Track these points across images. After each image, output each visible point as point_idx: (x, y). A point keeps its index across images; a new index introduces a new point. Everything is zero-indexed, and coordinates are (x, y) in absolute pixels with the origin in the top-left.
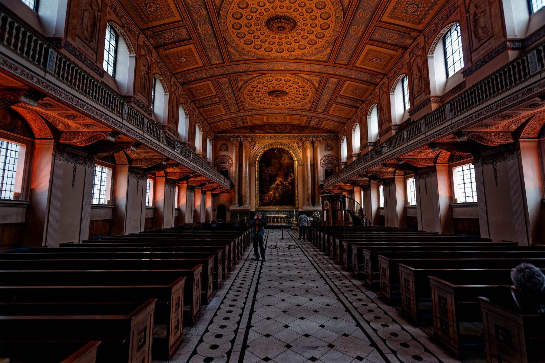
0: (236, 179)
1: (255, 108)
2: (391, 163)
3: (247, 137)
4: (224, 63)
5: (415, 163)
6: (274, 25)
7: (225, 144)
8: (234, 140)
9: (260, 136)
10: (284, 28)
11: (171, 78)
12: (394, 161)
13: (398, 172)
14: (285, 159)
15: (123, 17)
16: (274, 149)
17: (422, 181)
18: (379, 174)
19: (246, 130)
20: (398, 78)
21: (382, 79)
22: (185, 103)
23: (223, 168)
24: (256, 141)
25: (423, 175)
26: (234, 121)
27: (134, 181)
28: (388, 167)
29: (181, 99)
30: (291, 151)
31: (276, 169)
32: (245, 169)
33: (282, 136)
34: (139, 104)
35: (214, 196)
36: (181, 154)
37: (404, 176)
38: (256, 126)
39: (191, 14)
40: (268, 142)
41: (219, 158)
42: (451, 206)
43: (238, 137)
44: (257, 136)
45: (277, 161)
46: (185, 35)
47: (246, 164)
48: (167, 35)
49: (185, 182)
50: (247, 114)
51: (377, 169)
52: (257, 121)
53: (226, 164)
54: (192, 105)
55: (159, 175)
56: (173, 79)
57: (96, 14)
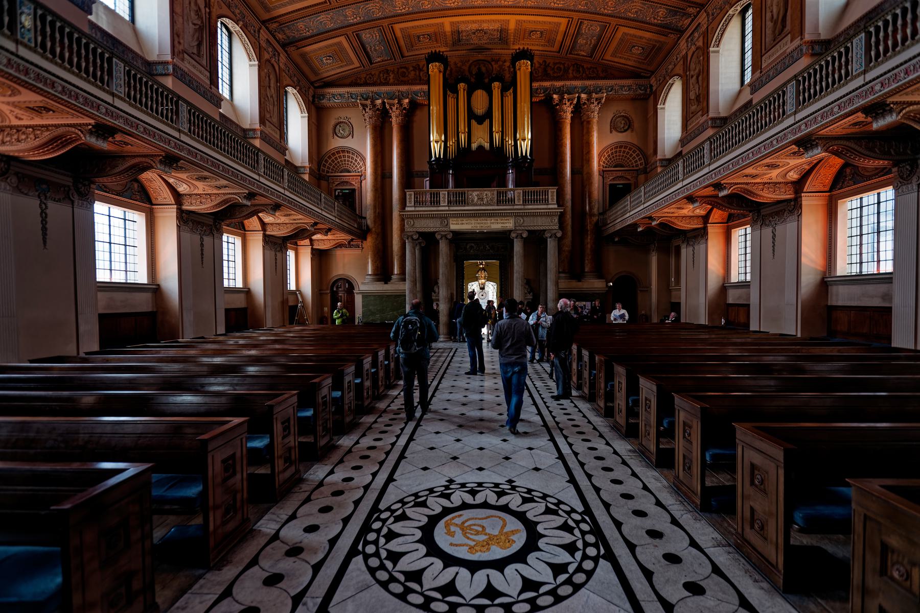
2: (705, 194)
5: (757, 195)
11: (259, 31)
12: (710, 191)
13: (717, 215)
17: (767, 231)
18: (676, 221)
20: (730, 12)
21: (696, 17)
25: (771, 219)
27: (193, 238)
28: (696, 205)
29: (288, 79)
37: (727, 223)
42: (826, 282)
49: (307, 242)
51: (672, 210)
55: (251, 228)
56: (264, 35)
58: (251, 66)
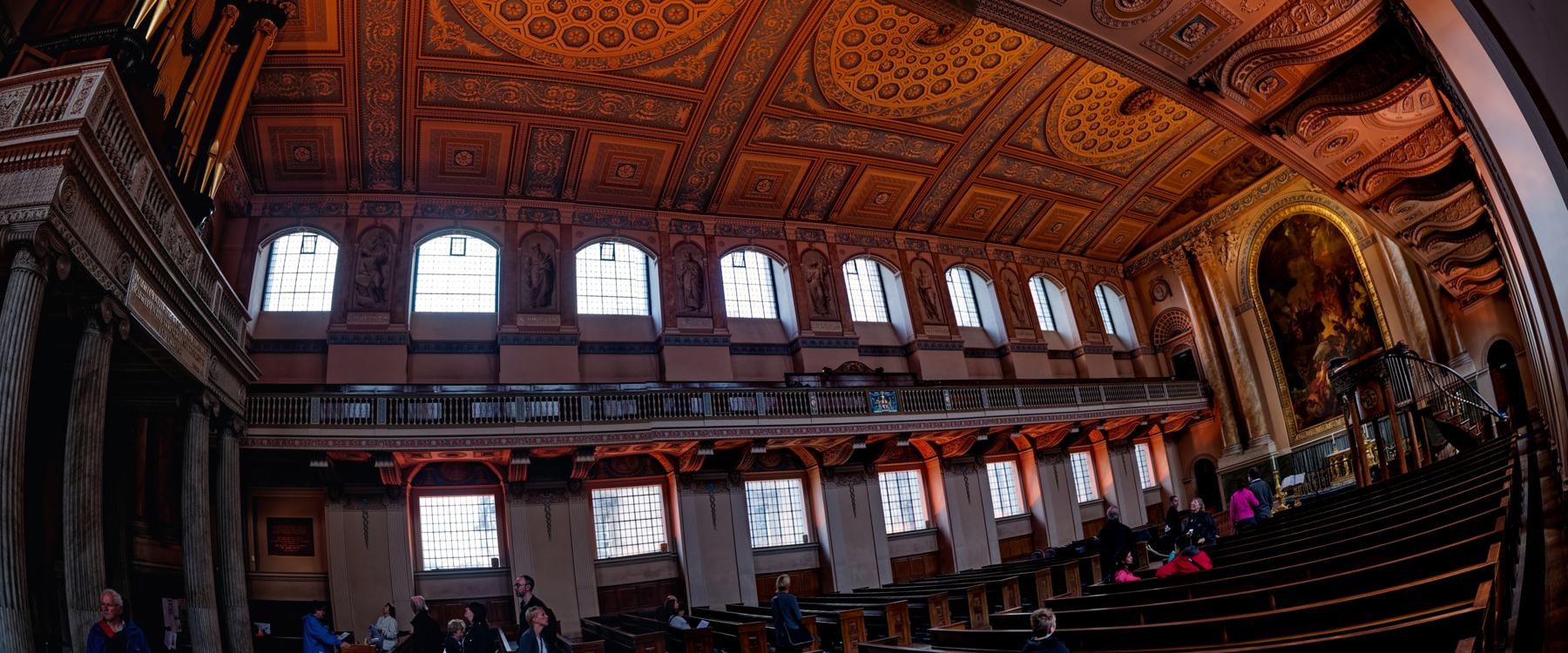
0: (1213, 371)
1: (1146, 156)
3: (1196, 234)
7: (1157, 279)
8: (1170, 258)
9: (1224, 211)
14: (1320, 245)
16: (1279, 228)
19: (1185, 212)
22: (964, 259)
23: (1177, 348)
24: (1223, 230)
26: (1135, 210)
30: (1326, 212)
31: (1311, 288)
32: (1229, 329)
33: (1278, 178)
34: (817, 341)
35: (1168, 439)
38: (1203, 187)
39: (813, 145)
40: (1254, 215)
41: (1159, 326)
43: (1177, 242)
44: (1217, 215)
45: (1302, 261)
47: (1224, 312)
50: (1142, 180)
52: (1191, 182)
53: (1180, 332)
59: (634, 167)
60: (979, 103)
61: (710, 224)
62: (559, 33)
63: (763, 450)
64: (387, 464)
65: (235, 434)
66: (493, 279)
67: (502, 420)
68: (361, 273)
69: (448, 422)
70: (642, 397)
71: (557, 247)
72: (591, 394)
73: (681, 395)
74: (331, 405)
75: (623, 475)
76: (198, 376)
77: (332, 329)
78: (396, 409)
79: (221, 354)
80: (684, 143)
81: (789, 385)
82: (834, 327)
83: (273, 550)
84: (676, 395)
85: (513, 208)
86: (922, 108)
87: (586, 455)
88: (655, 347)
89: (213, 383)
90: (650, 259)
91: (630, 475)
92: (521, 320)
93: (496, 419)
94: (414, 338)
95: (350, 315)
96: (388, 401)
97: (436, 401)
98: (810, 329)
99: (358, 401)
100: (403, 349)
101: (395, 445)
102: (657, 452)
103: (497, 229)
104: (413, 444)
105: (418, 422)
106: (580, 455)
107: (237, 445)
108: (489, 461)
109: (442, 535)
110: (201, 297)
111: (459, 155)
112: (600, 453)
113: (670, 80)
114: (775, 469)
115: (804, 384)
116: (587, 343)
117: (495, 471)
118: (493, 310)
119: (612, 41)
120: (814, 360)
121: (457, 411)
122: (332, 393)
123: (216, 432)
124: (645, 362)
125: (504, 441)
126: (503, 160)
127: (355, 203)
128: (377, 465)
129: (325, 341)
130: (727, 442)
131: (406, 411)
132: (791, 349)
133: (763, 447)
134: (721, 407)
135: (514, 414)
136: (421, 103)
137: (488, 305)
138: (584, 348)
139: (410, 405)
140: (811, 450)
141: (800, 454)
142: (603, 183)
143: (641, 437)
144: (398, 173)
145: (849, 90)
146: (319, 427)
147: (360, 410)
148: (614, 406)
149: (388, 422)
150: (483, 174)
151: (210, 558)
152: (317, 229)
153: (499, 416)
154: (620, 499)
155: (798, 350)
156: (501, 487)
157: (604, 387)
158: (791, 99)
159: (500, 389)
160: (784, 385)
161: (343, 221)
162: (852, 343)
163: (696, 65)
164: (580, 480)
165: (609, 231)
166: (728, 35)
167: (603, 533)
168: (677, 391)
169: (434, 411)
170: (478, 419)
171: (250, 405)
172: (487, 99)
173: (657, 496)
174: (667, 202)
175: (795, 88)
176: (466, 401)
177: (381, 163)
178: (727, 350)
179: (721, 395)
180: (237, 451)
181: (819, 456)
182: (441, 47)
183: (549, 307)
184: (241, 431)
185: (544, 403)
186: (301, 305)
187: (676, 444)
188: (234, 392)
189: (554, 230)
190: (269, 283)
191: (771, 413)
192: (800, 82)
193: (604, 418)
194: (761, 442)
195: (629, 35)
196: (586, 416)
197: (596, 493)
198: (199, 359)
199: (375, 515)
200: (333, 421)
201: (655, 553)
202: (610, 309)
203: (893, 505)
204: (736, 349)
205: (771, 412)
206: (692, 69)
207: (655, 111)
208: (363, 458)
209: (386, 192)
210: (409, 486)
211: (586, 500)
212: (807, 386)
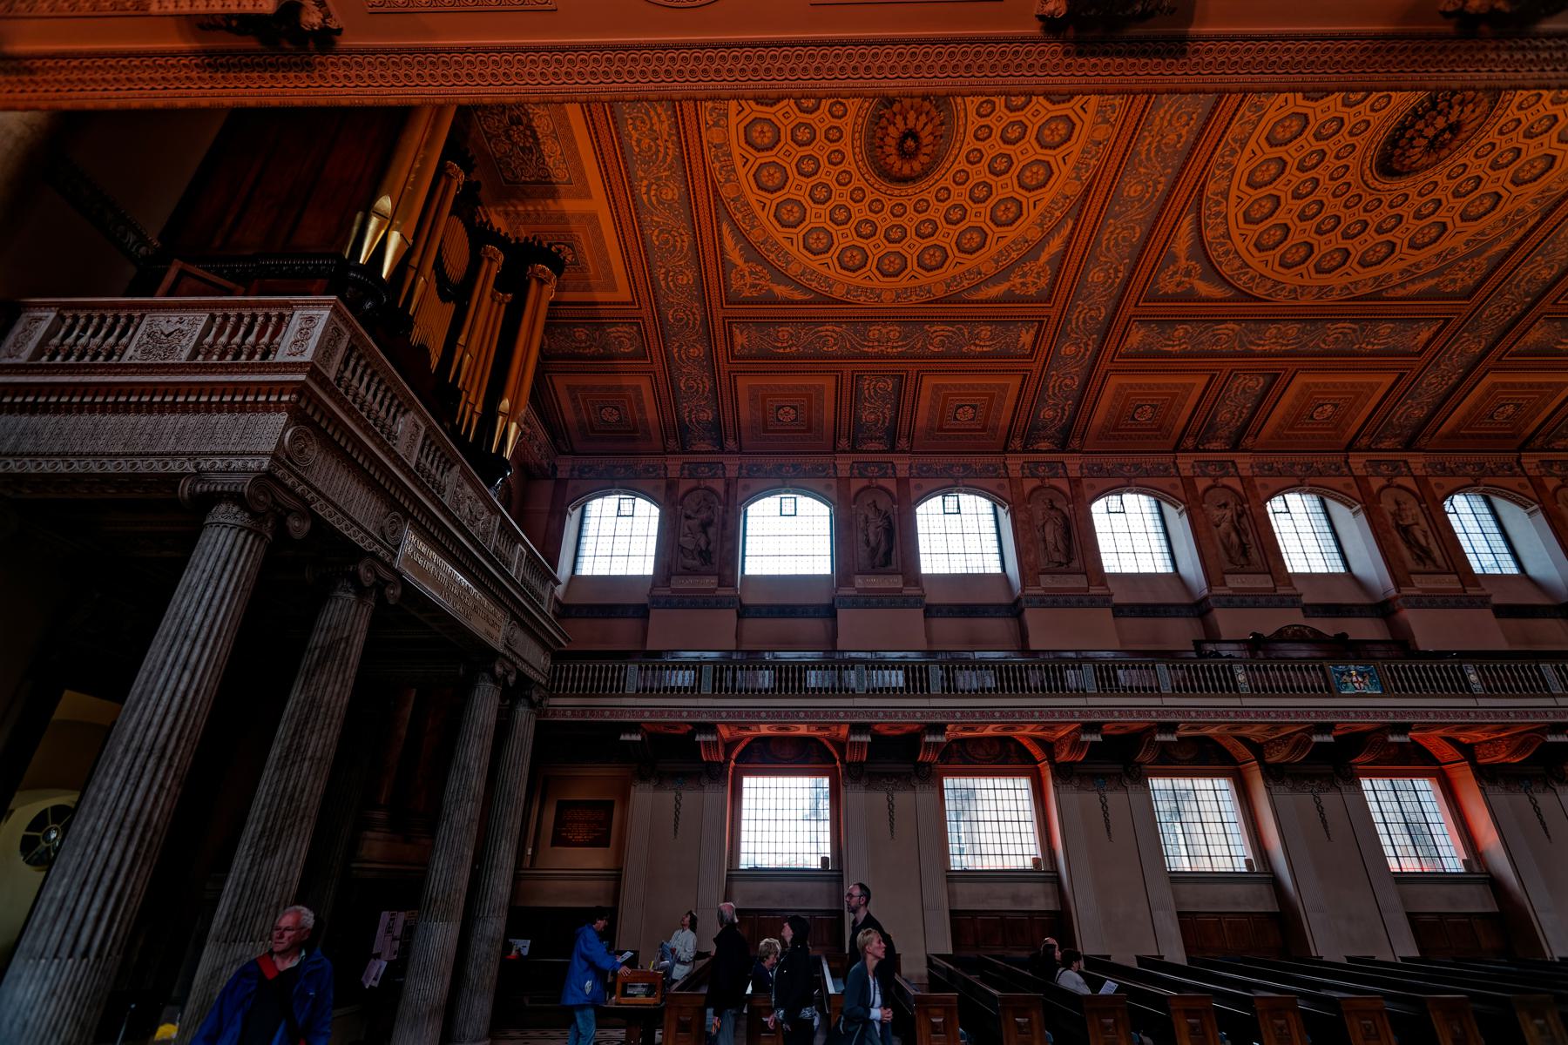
4: (1447, 321)
6: (1407, 162)
10: (1455, 128)
15: (1122, 465)
27: (1301, 800)
36: (1386, 693)
39: (1213, 354)
46: (1257, 384)
48: (1224, 415)
54: (1530, 461)
57: (1066, 510)
58: (1354, 513)
59: (974, 407)
60: (1505, 245)
61: (1074, 464)
62: (872, 263)
63: (1172, 738)
64: (709, 738)
65: (532, 705)
66: (828, 539)
67: (840, 690)
68: (685, 536)
69: (780, 692)
70: (1000, 668)
71: (894, 503)
72: (940, 663)
73: (1053, 667)
74: (650, 673)
75: (982, 762)
76: (492, 643)
77: (654, 593)
78: (723, 678)
79: (522, 619)
80: (1031, 371)
81: (1201, 655)
82: (1262, 582)
83: (559, 840)
84: (1046, 667)
85: (844, 463)
86: (1391, 276)
87: (935, 734)
88: (1014, 610)
89: (510, 650)
90: (999, 509)
91: (988, 761)
92: (859, 582)
93: (833, 689)
94: (744, 602)
95: (674, 579)
96: (715, 669)
97: (767, 668)
98: (1224, 584)
99: (681, 668)
100: (734, 612)
101: (720, 716)
102: (1024, 736)
103: (828, 487)
104: (740, 715)
105: (747, 691)
106: (930, 734)
107: (533, 717)
108: (824, 737)
109: (766, 817)
110: (501, 563)
111: (781, 411)
112: (952, 733)
113: (1009, 298)
114: (1190, 762)
115: (1224, 654)
116: (932, 605)
117: (833, 750)
118: (828, 572)
119: (934, 263)
120: (1231, 623)
121: (790, 680)
122: (653, 659)
123: (508, 702)
124: (997, 627)
125: (842, 714)
126: (828, 414)
127: (674, 465)
128: (698, 738)
129: (645, 605)
130: (1120, 725)
131: (734, 679)
132: (1199, 609)
133: (1173, 733)
134: (1107, 682)
135: (853, 684)
136: (734, 357)
137: (822, 565)
138: (931, 611)
139: (739, 674)
140: (1245, 740)
141: (1229, 744)
142: (940, 429)
143: (1002, 715)
144: (719, 433)
145: (1267, 272)
146: (636, 695)
147: (684, 678)
148: (967, 678)
149: (714, 691)
150: (809, 429)
151: (471, 853)
152: (635, 491)
153: (837, 685)
154: (978, 792)
155: (1210, 610)
156: (837, 768)
157: (955, 655)
158: (1171, 289)
159: (837, 656)
160: (1194, 655)
161: (663, 483)
162: (1293, 601)
163: (1038, 273)
164: (929, 764)
165: (951, 482)
166: (1075, 224)
167: (957, 834)
168: (1044, 661)
169: (765, 679)
170: (813, 689)
171: (555, 673)
172: (804, 347)
173: (1025, 792)
174: (1017, 443)
175: (1175, 273)
176: (800, 668)
177: (698, 423)
178: (1109, 611)
179: (1107, 667)
180: (532, 724)
181: (1258, 750)
182: (746, 293)
183: (889, 567)
184: (540, 702)
185: (887, 672)
186: (619, 569)
187: (1049, 727)
188: (536, 659)
189: (891, 485)
190: (582, 547)
191: (1178, 690)
192: (1183, 263)
193: (956, 691)
194: (1171, 727)
195: (952, 251)
196: (935, 688)
197: (948, 782)
198: (493, 625)
199: (689, 796)
200: (652, 690)
201: (1025, 871)
202: (958, 567)
203: (1394, 829)
204: (1120, 611)
205: (1179, 689)
206: (1034, 280)
207: (993, 339)
208: (682, 731)
209: (706, 453)
210: (733, 763)
211: (937, 791)
212: (1229, 656)
